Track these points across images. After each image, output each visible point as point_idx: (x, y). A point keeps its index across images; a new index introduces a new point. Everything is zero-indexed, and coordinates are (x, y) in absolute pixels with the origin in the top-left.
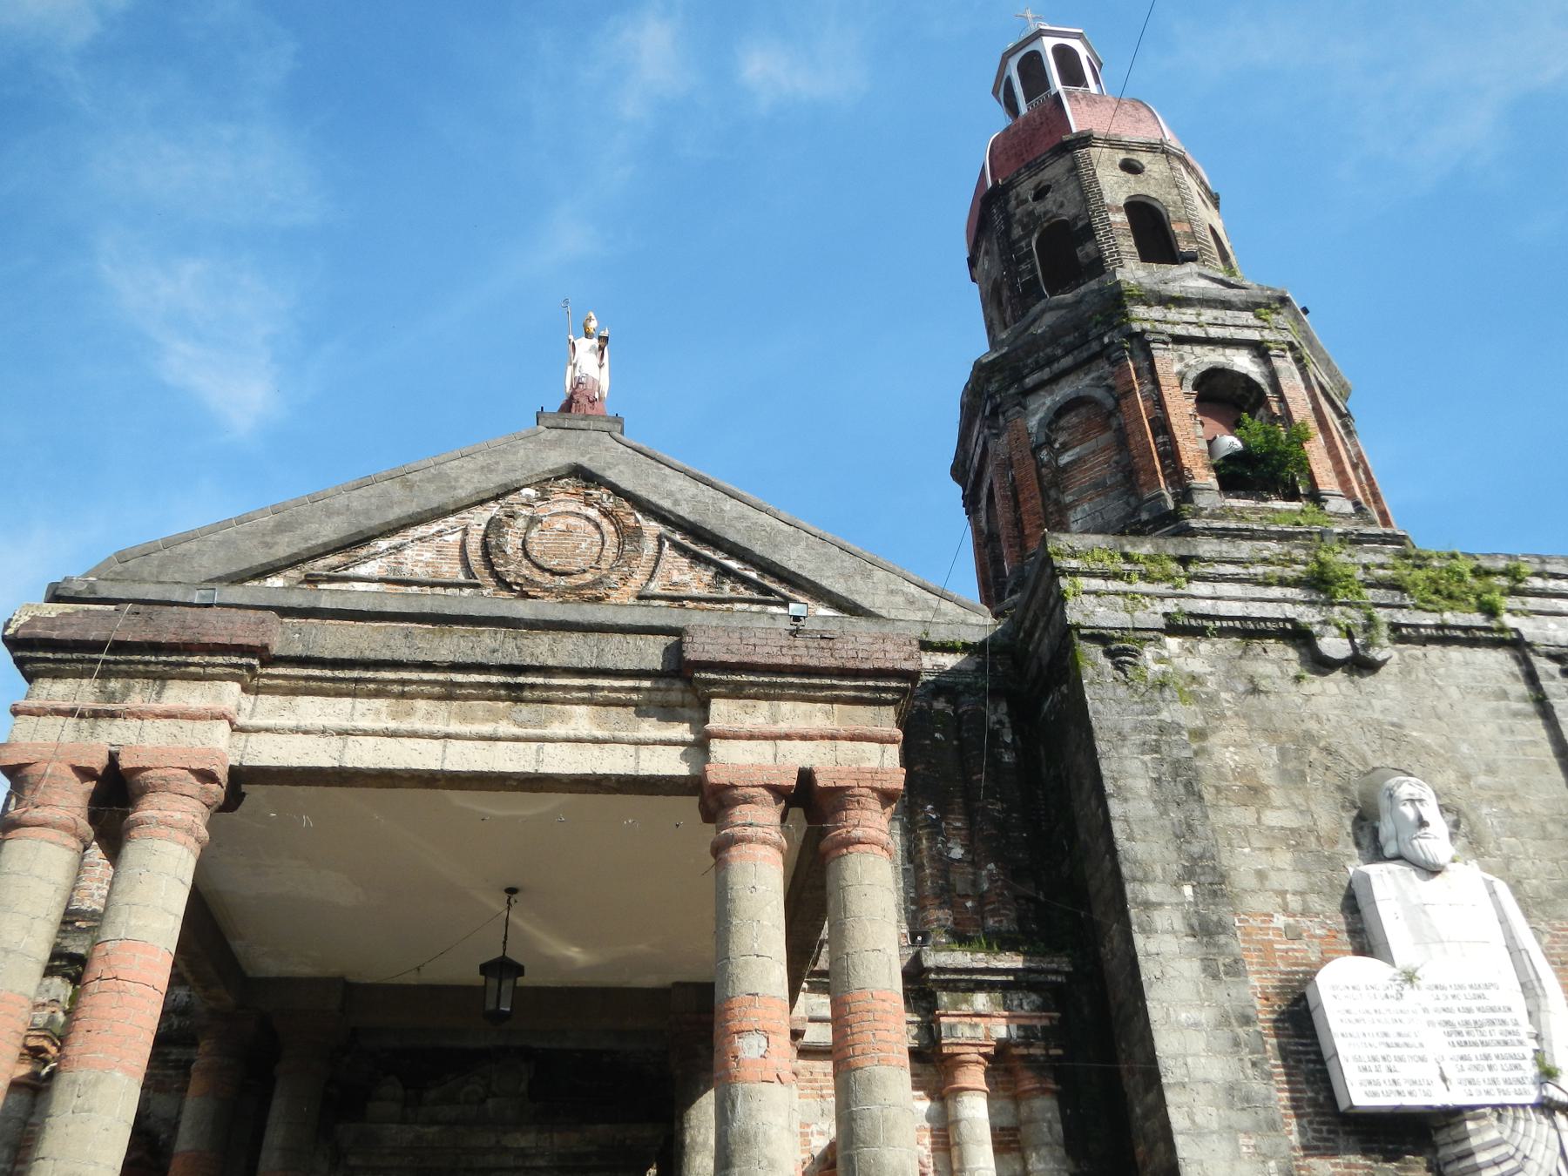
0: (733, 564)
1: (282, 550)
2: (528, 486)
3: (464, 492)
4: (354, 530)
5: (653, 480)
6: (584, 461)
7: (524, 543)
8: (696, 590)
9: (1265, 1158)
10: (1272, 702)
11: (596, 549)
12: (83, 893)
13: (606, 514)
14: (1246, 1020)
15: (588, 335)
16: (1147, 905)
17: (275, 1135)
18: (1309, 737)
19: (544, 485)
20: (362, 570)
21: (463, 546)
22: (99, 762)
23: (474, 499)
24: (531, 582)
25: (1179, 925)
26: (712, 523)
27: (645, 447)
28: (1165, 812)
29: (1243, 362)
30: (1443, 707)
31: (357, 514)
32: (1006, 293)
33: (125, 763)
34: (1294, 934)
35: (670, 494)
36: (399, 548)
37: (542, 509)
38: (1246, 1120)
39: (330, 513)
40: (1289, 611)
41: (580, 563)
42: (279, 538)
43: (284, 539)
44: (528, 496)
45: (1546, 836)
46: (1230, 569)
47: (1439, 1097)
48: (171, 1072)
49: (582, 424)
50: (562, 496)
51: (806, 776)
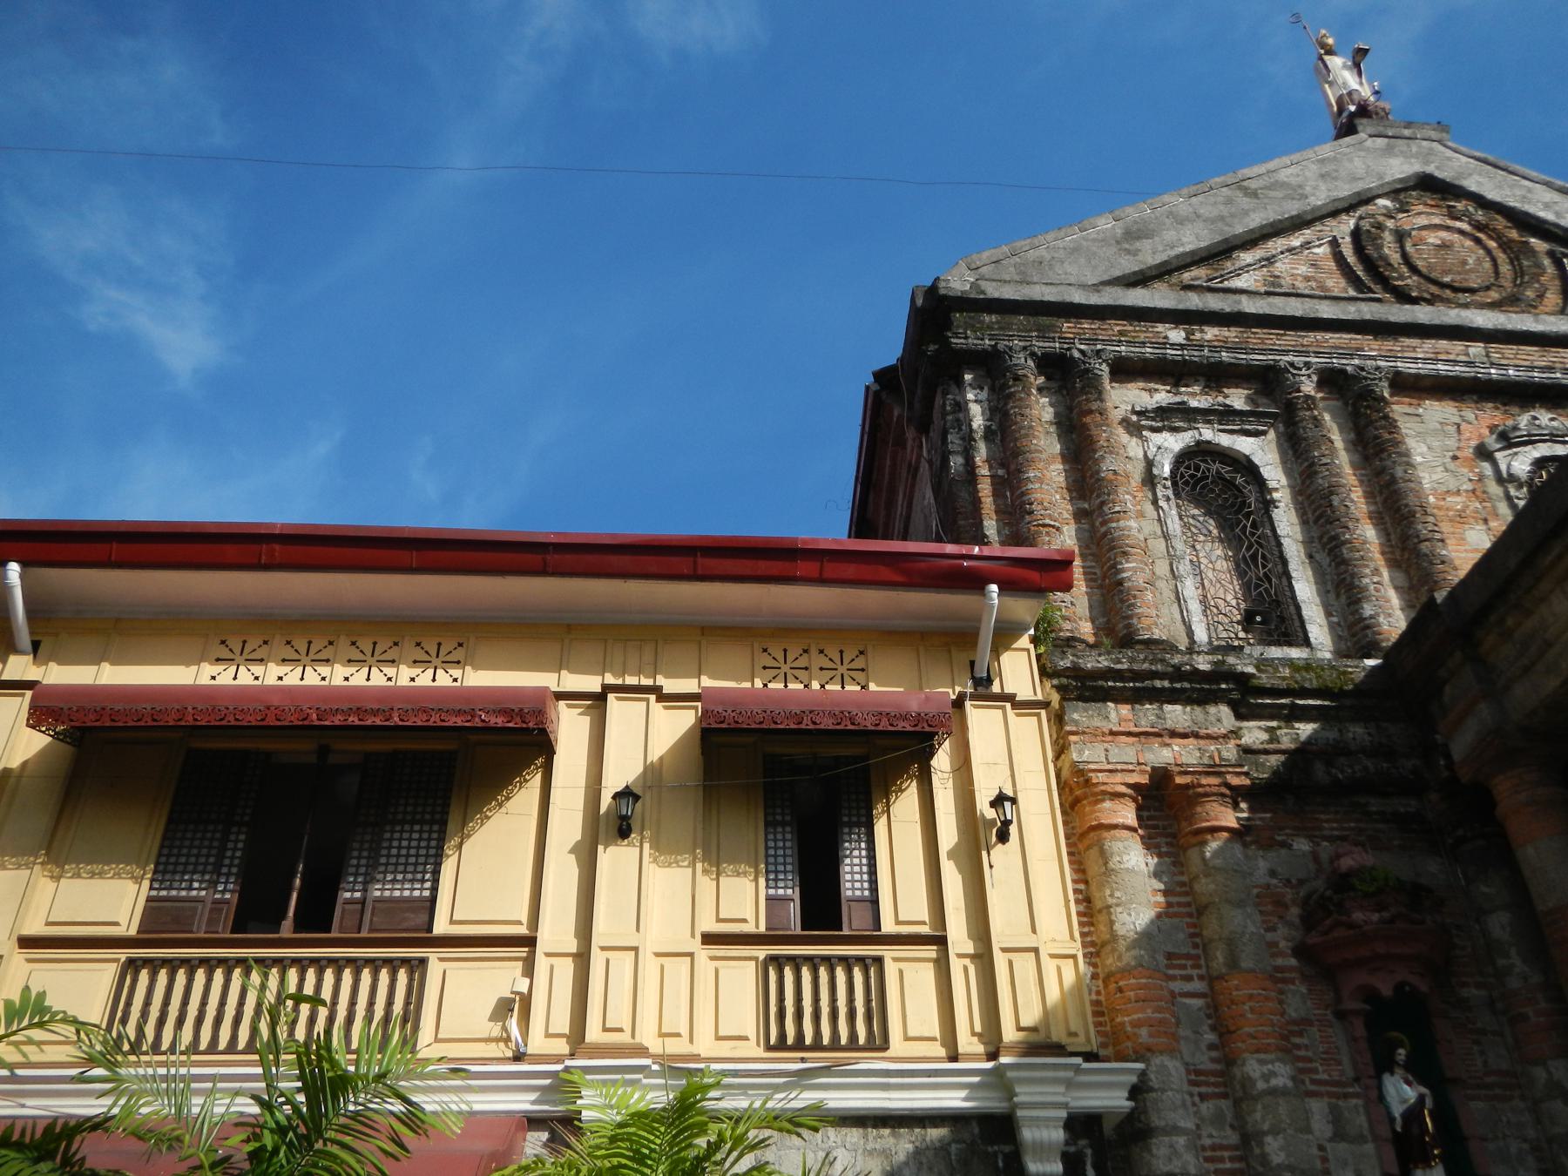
1: (1151, 254)
2: (1379, 196)
3: (1320, 197)
4: (1218, 238)
5: (1518, 192)
6: (1430, 169)
7: (1405, 256)
11: (1488, 265)
12: (1145, 622)
13: (1479, 227)
15: (1330, 52)
21: (1339, 257)
23: (1331, 208)
27: (1491, 158)
31: (1213, 221)
35: (1547, 206)
36: (1270, 260)
37: (1405, 222)
39: (1181, 221)
42: (1138, 244)
43: (1146, 245)
44: (1385, 207)
48: (1380, 826)
49: (1407, 132)
50: (1421, 208)
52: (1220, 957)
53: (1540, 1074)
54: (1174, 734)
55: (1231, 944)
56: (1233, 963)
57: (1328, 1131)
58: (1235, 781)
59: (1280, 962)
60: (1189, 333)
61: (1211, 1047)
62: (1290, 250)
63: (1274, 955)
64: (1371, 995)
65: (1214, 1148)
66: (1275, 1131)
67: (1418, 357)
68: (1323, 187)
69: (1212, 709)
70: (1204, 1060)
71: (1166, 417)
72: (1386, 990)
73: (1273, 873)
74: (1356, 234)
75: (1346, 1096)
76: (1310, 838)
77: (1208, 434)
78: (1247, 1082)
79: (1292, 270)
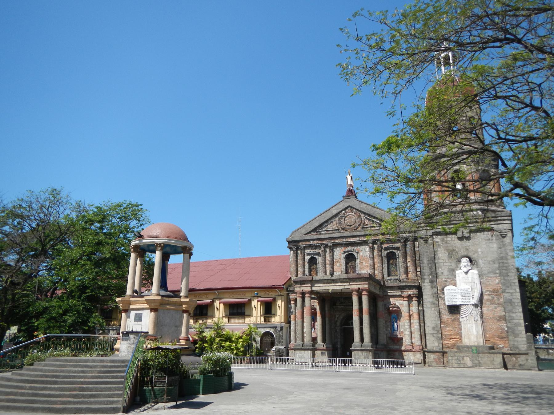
0: (374, 220)
1: (312, 228)
8: (369, 225)
10: (449, 245)
14: (435, 294)
16: (424, 279)
17: (326, 309)
18: (454, 250)
25: (428, 281)
26: (371, 213)
28: (428, 265)
30: (477, 243)
34: (446, 281)
45: (489, 264)
47: (458, 304)
51: (359, 288)
71: (308, 254)
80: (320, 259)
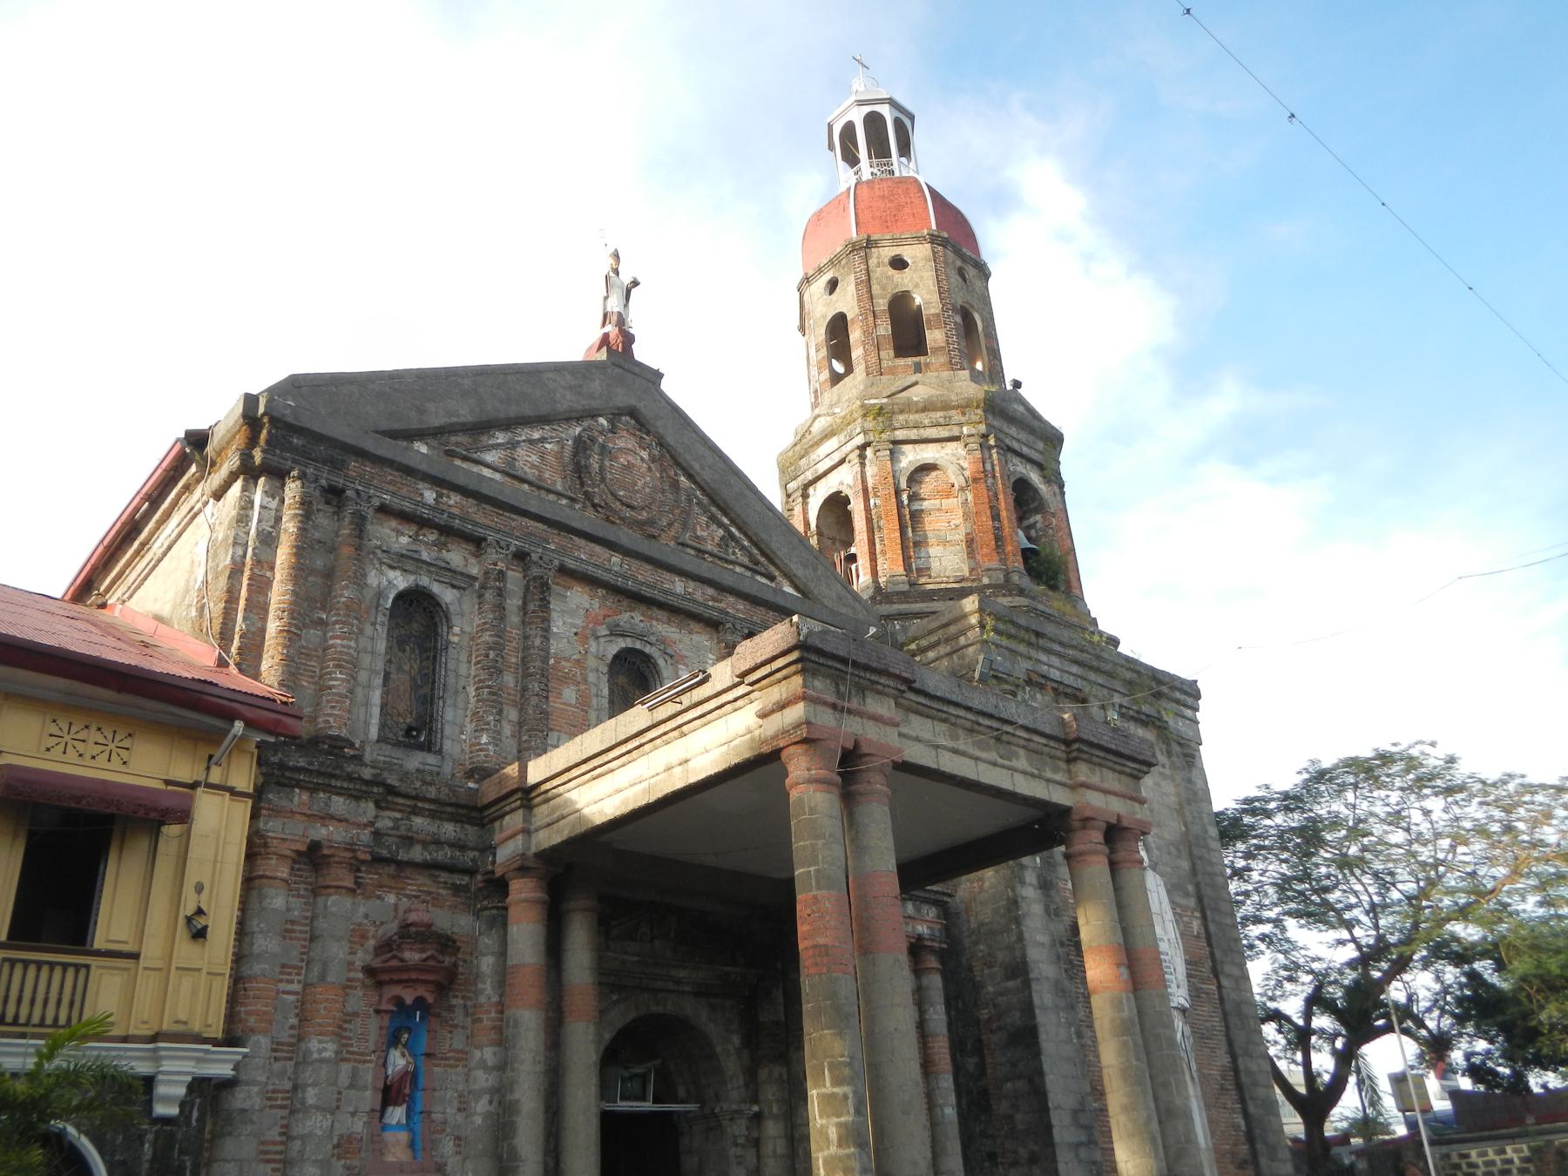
6: (641, 406)
7: (602, 468)
9: (1070, 1025)
19: (615, 416)
20: (490, 457)
22: (850, 745)
24: (612, 510)
29: (1034, 477)
32: (855, 335)
33: (865, 749)
38: (1062, 1003)
40: (1079, 684)
41: (638, 501)
46: (1057, 647)
52: (316, 970)
53: (477, 1054)
54: (332, 817)
55: (325, 965)
56: (322, 977)
57: (347, 1082)
58: (362, 857)
59: (352, 975)
60: (440, 496)
61: (292, 1027)
62: (531, 442)
63: (350, 970)
64: (399, 1001)
65: (274, 1091)
66: (314, 1085)
67: (584, 554)
68: (568, 396)
69: (363, 805)
70: (285, 1036)
71: (403, 561)
72: (409, 1001)
73: (366, 916)
74: (578, 440)
75: (365, 1062)
76: (397, 894)
77: (424, 581)
78: (309, 1052)
79: (526, 459)
80: (465, 622)
